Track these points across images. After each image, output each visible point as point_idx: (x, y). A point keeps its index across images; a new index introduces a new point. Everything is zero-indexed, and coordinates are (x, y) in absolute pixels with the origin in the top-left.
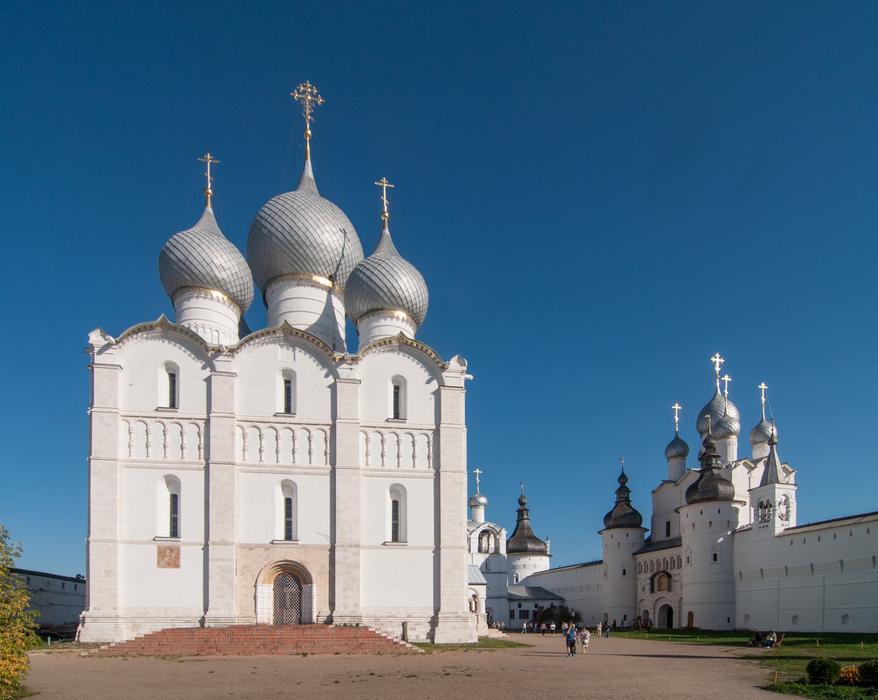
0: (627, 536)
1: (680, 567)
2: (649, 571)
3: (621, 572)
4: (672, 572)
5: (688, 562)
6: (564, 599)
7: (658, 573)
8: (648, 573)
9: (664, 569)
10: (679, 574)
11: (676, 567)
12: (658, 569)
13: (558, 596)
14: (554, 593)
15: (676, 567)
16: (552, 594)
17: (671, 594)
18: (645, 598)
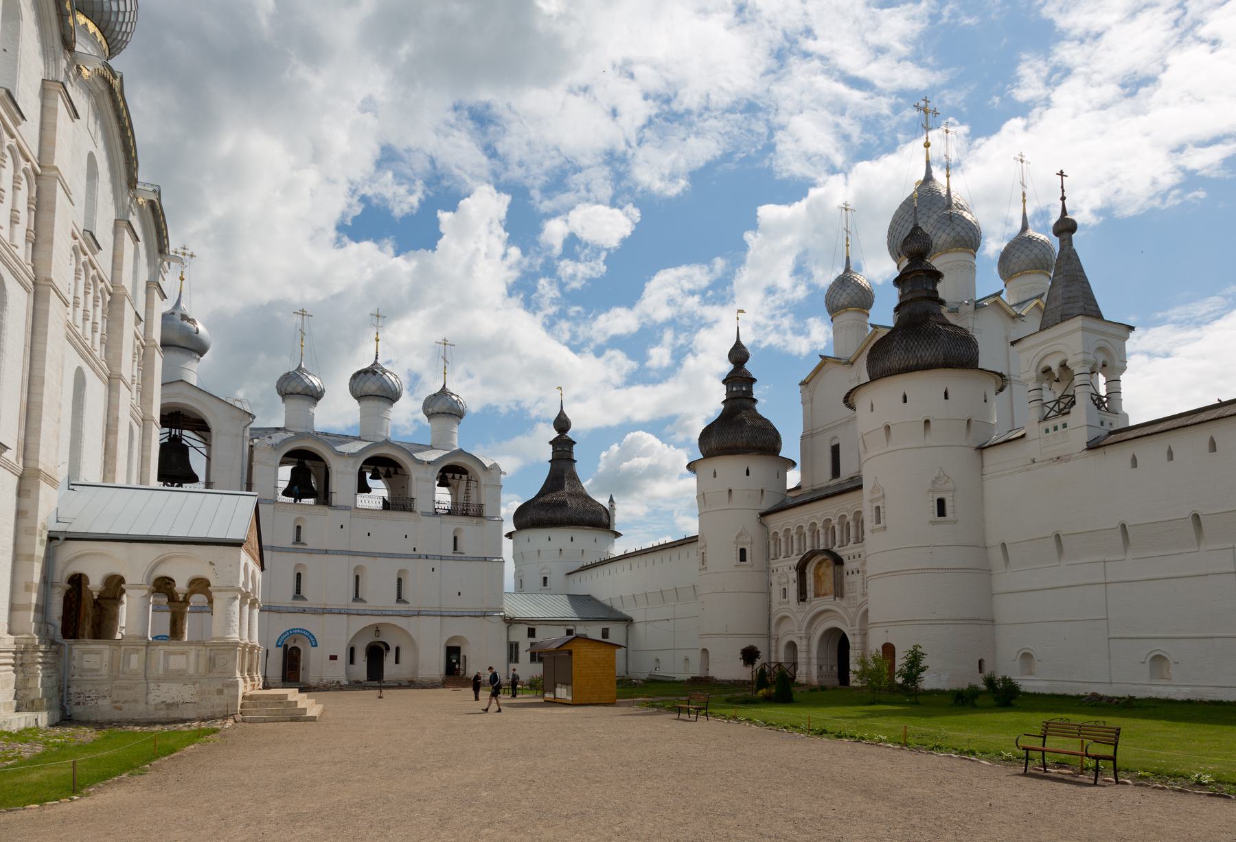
0: (748, 474)
1: (859, 539)
2: (795, 552)
5: (879, 522)
6: (631, 620)
7: (814, 553)
8: (794, 556)
9: (827, 544)
10: (860, 556)
11: (852, 540)
12: (813, 546)
14: (615, 607)
15: (852, 540)
16: (611, 609)
17: (844, 603)
18: (791, 616)
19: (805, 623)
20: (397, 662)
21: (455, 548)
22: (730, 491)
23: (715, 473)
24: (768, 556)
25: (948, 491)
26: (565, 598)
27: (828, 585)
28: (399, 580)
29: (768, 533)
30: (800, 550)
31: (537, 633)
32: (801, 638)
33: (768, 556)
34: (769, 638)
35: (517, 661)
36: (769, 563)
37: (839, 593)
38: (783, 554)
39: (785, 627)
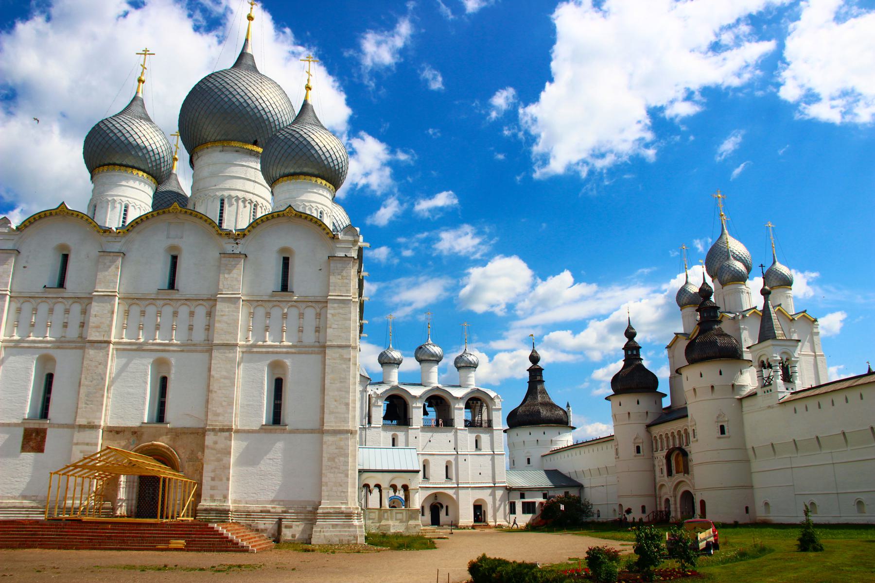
2: (666, 448)
3: (634, 449)
4: (687, 449)
5: (694, 437)
9: (680, 444)
13: (576, 481)
14: (572, 477)
17: (689, 477)
19: (673, 488)
20: (447, 514)
21: (477, 447)
22: (629, 413)
23: (620, 403)
24: (653, 449)
25: (725, 421)
26: (543, 473)
27: (681, 468)
28: (447, 467)
29: (651, 437)
30: (668, 446)
31: (526, 495)
32: (671, 497)
33: (653, 449)
34: (656, 497)
35: (514, 513)
36: (653, 454)
37: (686, 471)
38: (660, 449)
39: (664, 490)
